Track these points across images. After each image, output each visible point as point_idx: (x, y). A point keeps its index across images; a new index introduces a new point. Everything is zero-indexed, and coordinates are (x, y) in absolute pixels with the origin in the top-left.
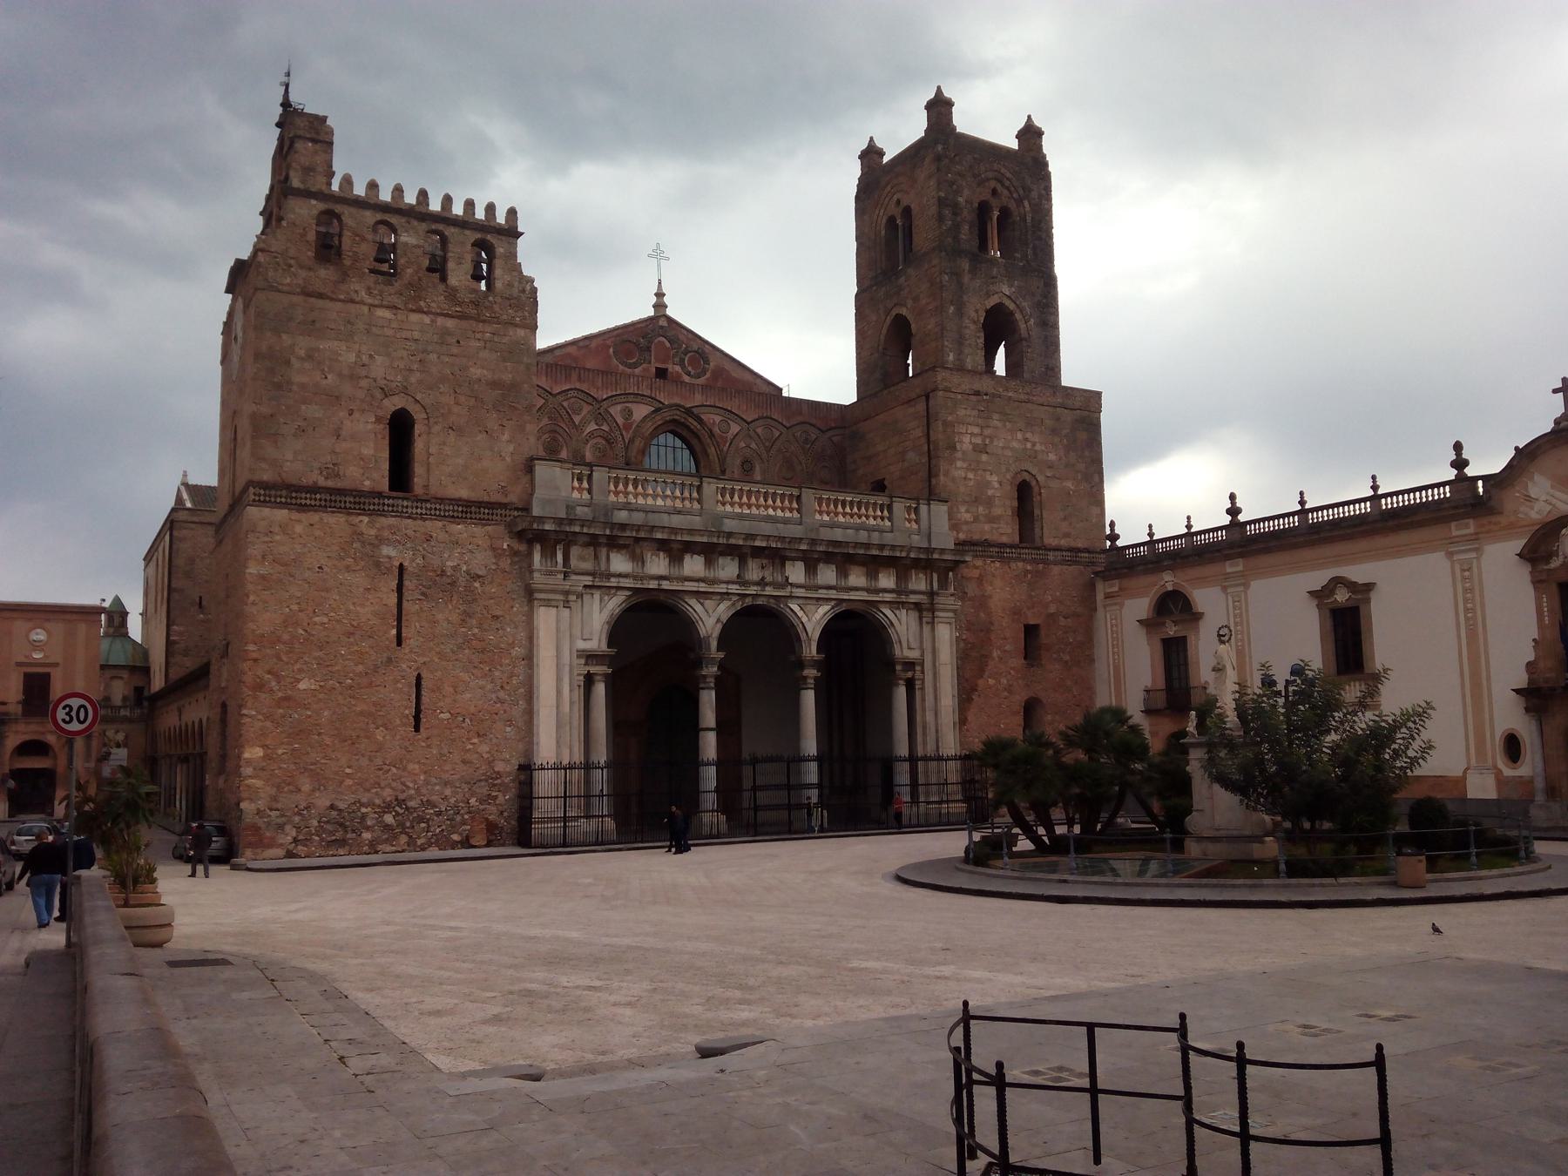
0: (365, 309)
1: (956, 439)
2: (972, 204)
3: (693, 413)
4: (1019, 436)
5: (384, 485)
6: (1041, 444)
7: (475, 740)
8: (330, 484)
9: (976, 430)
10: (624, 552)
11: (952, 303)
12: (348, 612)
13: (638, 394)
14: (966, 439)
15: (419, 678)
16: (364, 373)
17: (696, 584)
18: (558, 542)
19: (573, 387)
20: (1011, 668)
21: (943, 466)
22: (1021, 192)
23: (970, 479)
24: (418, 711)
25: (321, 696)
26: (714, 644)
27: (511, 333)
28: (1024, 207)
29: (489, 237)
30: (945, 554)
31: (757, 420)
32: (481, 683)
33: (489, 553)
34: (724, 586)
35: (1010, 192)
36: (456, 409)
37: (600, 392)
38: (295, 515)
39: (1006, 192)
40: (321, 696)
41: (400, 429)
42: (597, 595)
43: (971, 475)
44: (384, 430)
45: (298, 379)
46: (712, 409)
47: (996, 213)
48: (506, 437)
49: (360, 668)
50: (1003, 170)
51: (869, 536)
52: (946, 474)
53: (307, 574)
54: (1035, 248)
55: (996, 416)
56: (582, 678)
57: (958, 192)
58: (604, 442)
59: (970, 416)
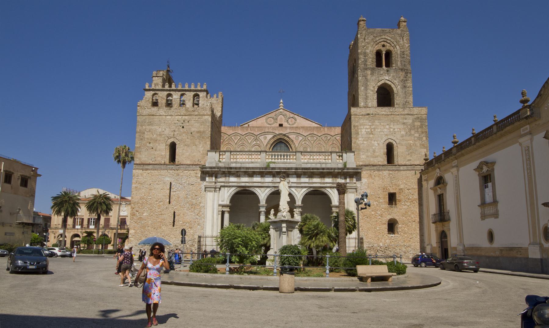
0: (164, 117)
1: (359, 131)
2: (373, 52)
4: (387, 127)
5: (167, 161)
6: (397, 129)
7: (189, 229)
8: (153, 163)
9: (368, 127)
10: (234, 175)
11: (363, 86)
12: (157, 195)
14: (363, 130)
15: (174, 213)
16: (163, 133)
17: (257, 184)
18: (214, 174)
20: (382, 208)
21: (353, 140)
22: (395, 43)
23: (365, 144)
24: (174, 221)
25: (149, 217)
26: (265, 202)
27: (204, 118)
29: (198, 93)
32: (192, 213)
33: (195, 178)
34: (267, 184)
35: (391, 45)
36: (187, 140)
38: (144, 171)
39: (388, 45)
40: (149, 217)
41: (173, 147)
42: (226, 188)
43: (365, 142)
44: (168, 148)
45: (146, 137)
47: (384, 52)
48: (201, 146)
49: (159, 210)
50: (387, 37)
51: (321, 166)
52: (355, 143)
53: (147, 186)
55: (376, 121)
56: (221, 212)
57: (367, 48)
58: (258, 146)
59: (365, 122)
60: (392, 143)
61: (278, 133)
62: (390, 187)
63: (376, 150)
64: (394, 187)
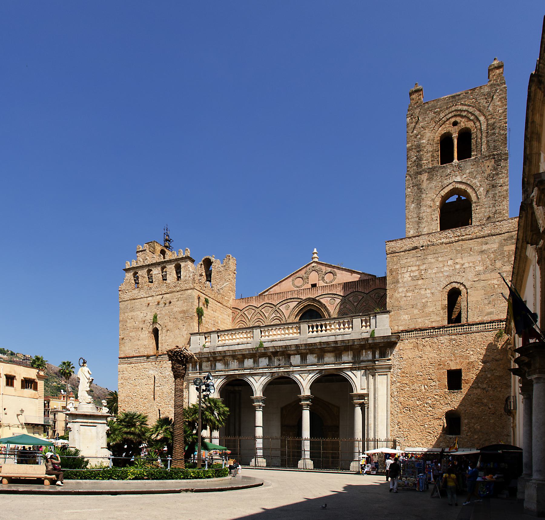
3: (316, 300)
13: (292, 298)
19: (265, 302)
31: (349, 294)
37: (276, 301)
46: (326, 296)
58: (278, 321)
60: (458, 289)
61: (304, 298)
62: (451, 360)
64: (458, 361)
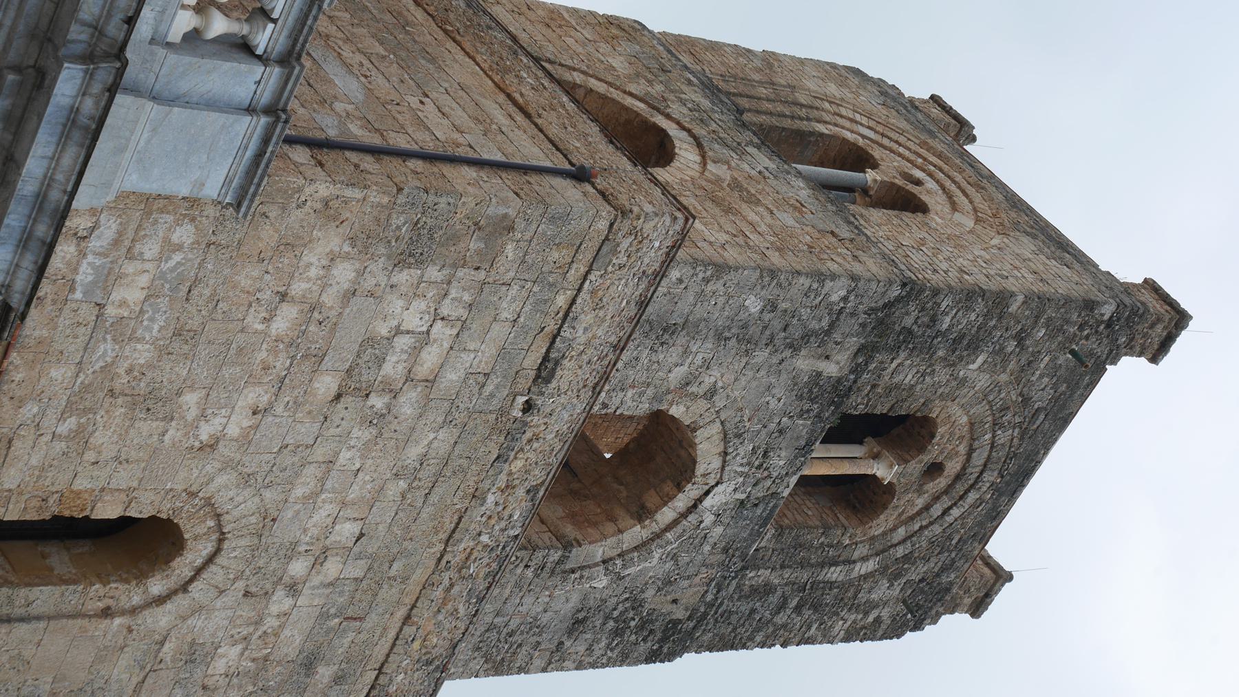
28: (864, 559)
30: (64, 138)
50: (972, 497)
52: (328, 211)
54: (768, 589)
55: (446, 436)
63: (147, 427)
